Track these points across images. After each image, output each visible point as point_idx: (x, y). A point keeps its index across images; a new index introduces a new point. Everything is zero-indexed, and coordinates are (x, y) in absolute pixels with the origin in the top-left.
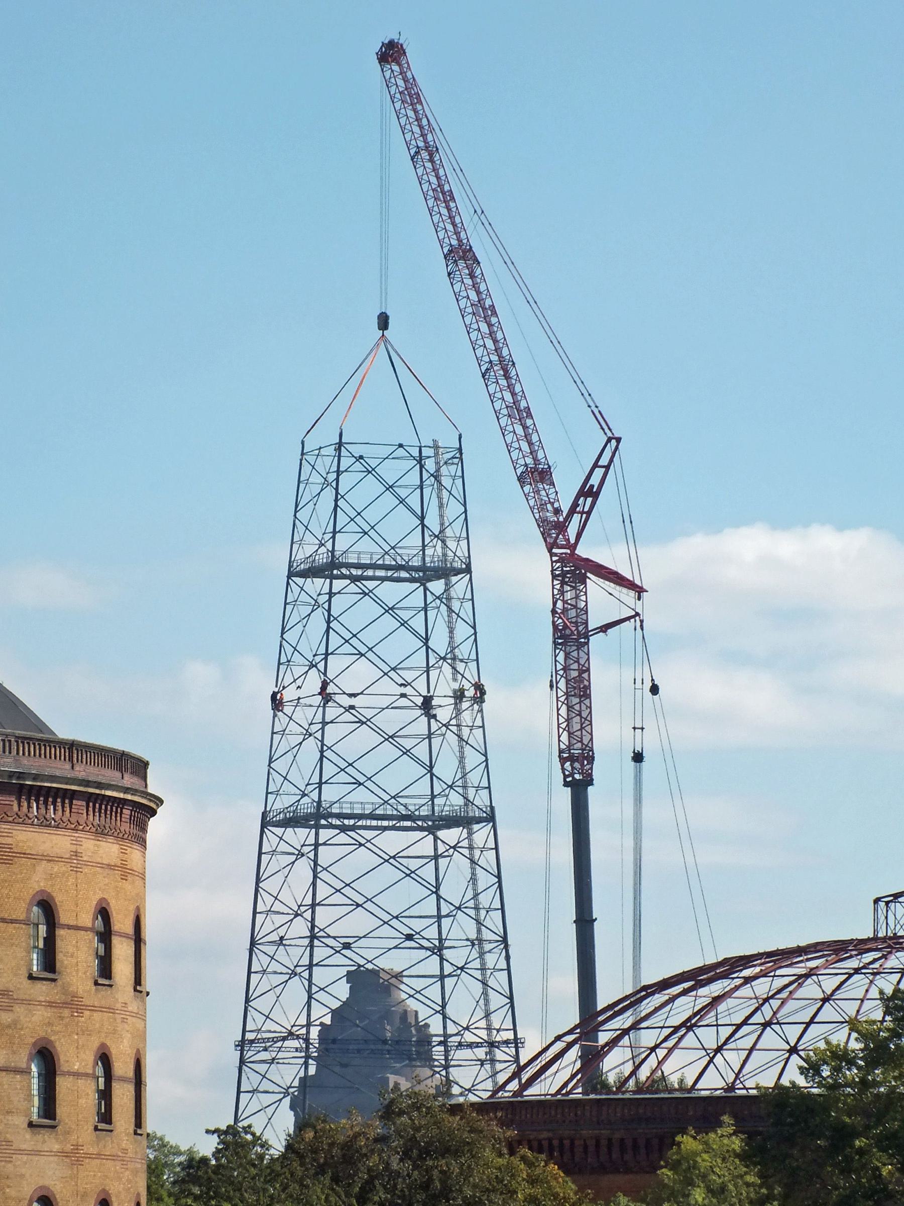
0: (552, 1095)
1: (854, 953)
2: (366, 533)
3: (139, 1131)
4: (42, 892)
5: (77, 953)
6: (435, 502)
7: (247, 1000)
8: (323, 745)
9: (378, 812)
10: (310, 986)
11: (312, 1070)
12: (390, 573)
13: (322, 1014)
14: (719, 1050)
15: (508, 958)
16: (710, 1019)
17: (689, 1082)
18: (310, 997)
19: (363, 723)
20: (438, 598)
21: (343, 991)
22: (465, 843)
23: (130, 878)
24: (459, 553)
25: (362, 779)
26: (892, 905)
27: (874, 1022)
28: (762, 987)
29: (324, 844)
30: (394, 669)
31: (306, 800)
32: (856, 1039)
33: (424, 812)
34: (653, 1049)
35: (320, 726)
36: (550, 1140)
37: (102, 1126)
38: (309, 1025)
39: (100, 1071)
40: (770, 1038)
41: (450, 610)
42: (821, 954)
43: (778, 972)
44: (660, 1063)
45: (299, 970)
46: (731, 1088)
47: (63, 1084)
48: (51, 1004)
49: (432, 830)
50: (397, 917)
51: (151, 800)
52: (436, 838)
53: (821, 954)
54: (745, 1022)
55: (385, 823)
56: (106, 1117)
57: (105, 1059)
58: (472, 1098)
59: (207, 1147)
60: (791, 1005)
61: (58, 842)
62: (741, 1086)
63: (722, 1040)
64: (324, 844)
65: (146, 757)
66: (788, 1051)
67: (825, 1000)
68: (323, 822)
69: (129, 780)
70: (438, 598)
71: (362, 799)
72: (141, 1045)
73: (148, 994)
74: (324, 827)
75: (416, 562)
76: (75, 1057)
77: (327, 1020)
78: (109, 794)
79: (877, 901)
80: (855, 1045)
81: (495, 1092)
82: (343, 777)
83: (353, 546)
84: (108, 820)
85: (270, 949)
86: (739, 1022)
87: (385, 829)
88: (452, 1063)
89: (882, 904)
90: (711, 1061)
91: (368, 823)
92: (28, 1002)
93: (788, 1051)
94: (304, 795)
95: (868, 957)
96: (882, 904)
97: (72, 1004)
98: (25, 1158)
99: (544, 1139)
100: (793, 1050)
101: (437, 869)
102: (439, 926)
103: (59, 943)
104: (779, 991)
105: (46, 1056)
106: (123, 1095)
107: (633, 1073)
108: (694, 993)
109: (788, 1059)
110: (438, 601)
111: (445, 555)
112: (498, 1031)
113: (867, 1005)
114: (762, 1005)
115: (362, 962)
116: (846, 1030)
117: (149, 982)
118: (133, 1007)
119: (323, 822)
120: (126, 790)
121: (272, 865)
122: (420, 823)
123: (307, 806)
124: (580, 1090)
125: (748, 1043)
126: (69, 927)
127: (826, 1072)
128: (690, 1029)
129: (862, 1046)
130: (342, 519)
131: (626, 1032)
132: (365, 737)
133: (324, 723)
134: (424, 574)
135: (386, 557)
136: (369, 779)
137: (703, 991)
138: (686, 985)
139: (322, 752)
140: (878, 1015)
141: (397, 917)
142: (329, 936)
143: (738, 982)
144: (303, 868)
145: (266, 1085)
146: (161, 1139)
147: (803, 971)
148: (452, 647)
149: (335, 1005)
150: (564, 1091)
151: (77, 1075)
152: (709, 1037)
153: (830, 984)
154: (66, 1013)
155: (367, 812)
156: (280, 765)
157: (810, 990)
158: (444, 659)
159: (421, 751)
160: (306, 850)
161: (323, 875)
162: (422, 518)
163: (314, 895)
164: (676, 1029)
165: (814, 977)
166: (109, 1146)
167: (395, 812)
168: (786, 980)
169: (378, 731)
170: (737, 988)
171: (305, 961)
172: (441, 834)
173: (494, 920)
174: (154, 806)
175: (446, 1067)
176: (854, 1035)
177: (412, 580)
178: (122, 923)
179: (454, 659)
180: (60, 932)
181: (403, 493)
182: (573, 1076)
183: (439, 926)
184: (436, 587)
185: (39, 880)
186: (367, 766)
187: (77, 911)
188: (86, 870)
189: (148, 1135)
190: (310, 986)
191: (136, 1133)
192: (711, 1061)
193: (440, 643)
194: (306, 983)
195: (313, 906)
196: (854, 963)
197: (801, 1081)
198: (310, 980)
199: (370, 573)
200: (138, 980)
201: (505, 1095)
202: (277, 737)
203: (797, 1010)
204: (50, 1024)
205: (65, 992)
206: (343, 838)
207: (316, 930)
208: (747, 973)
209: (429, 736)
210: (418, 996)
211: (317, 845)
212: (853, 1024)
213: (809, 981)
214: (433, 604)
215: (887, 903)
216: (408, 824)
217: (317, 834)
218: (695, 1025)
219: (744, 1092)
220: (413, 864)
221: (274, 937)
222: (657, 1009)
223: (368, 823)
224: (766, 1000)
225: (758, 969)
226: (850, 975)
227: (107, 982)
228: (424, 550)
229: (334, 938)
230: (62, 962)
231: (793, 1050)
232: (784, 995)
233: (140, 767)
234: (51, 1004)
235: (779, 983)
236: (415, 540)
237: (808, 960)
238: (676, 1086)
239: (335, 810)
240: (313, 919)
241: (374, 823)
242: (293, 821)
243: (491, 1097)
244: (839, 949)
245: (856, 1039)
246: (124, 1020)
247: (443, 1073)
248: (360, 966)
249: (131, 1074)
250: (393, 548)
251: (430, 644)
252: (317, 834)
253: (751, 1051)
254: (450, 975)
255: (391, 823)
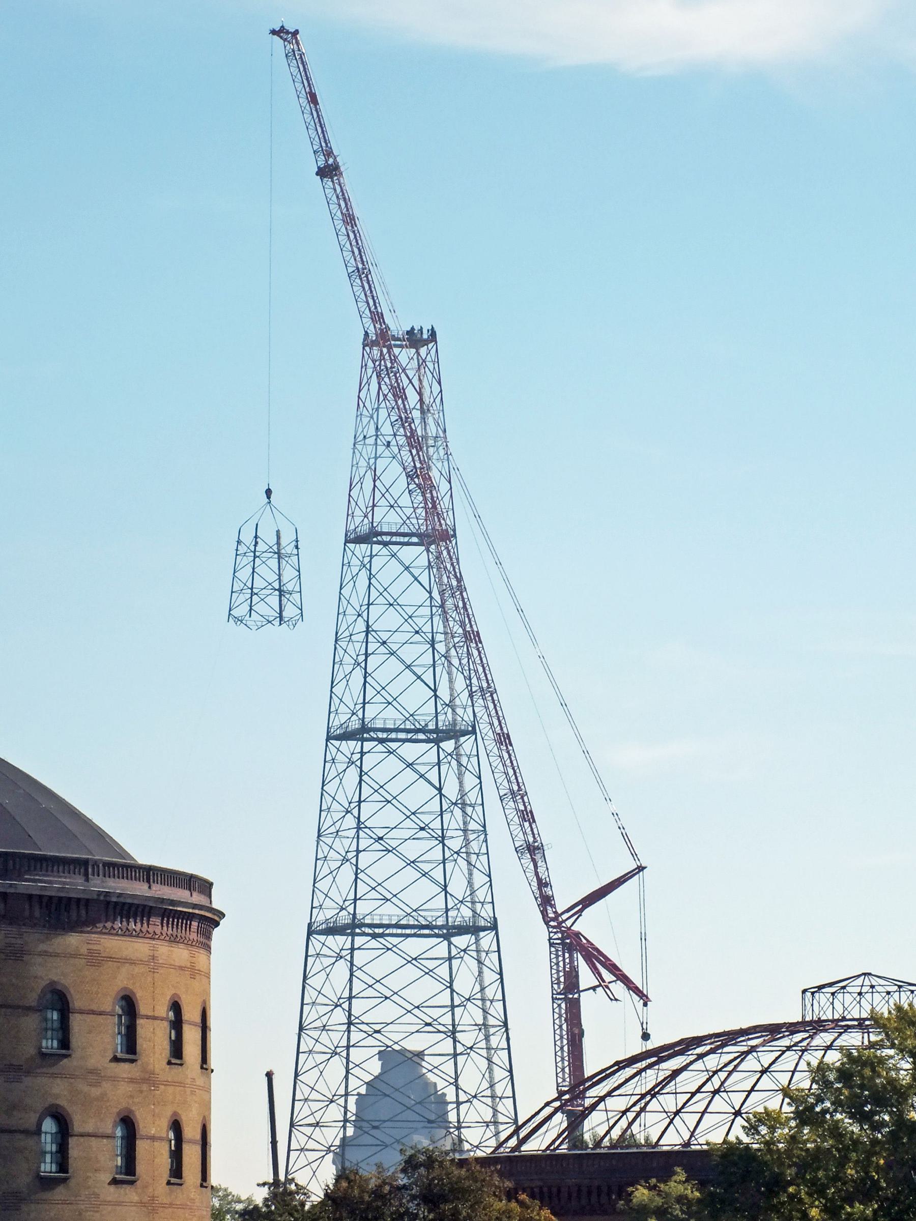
0: (543, 1151)
1: (787, 1033)
2: (390, 703)
3: (204, 1184)
4: (125, 989)
5: (154, 1037)
6: (445, 676)
7: (296, 1075)
8: (357, 868)
9: (402, 922)
10: (348, 1063)
11: (350, 1131)
12: (410, 736)
13: (357, 1085)
14: (677, 1113)
15: (508, 1039)
16: (670, 1088)
17: (655, 1140)
18: (348, 1072)
19: (389, 851)
20: (449, 754)
21: (375, 1067)
22: (473, 947)
23: (198, 977)
24: (466, 718)
25: (389, 896)
26: (817, 995)
27: (803, 1090)
28: (712, 1062)
29: (359, 948)
30: (413, 814)
31: (344, 913)
32: (789, 1104)
33: (440, 922)
34: (624, 1113)
35: (355, 853)
36: (541, 1188)
37: (173, 1180)
38: (347, 1094)
39: (171, 1135)
40: (719, 1103)
41: (460, 764)
42: (759, 1034)
43: (726, 1049)
44: (630, 1124)
45: (338, 1050)
46: (687, 1144)
47: (141, 1146)
48: (132, 1081)
49: (447, 937)
50: (418, 1007)
51: (214, 914)
52: (450, 943)
53: (759, 1034)
54: (698, 1091)
55: (408, 931)
56: (177, 1171)
57: (176, 1126)
58: (479, 1154)
59: (260, 1196)
60: (735, 1076)
61: (138, 948)
62: (695, 1142)
63: (680, 1106)
64: (359, 948)
65: (211, 880)
66: (733, 1114)
67: (764, 1072)
68: (358, 931)
69: (197, 898)
70: (449, 754)
71: (389, 913)
72: (206, 1114)
73: (212, 1071)
74: (359, 935)
75: (431, 726)
76: (153, 1124)
77: (363, 1090)
78: (182, 909)
79: (804, 991)
80: (788, 1109)
81: (497, 1148)
82: (373, 894)
83: (381, 715)
84: (179, 930)
85: (315, 1034)
86: (693, 1090)
87: (408, 936)
88: (463, 1125)
89: (808, 994)
90: (671, 1122)
91: (395, 931)
92: (114, 1079)
93: (733, 1114)
94: (342, 909)
95: (798, 1037)
96: (808, 994)
97: (149, 1079)
98: (110, 1208)
99: (536, 1187)
100: (738, 1113)
101: (451, 968)
102: (453, 1014)
103: (139, 1029)
104: (726, 1065)
105: (128, 1123)
106: (191, 1155)
107: (608, 1132)
108: (657, 1067)
109: (733, 1120)
110: (449, 757)
111: (454, 720)
112: (500, 1098)
113: (797, 1076)
114: (713, 1076)
115: (390, 1043)
116: (781, 1097)
117: (214, 1061)
118: (200, 1082)
119: (358, 931)
120: (195, 906)
121: (315, 966)
122: (436, 931)
123: (344, 918)
124: (564, 1146)
125: (701, 1107)
126: (148, 1017)
127: (764, 1130)
128: (653, 1096)
129: (793, 1109)
130: (370, 693)
131: (602, 1099)
132: (392, 862)
133: (358, 851)
134: (438, 736)
135: (407, 722)
136: (395, 896)
137: (663, 1065)
138: (650, 1061)
139: (356, 874)
140: (806, 1084)
141: (418, 1007)
142: (363, 1023)
143: (692, 1058)
144: (342, 968)
145: (311, 1145)
146: (226, 1190)
147: (745, 1049)
148: (463, 794)
149: (368, 1078)
150: (552, 1148)
151: (153, 1138)
152: (669, 1102)
153: (767, 1059)
154: (145, 1087)
155: (394, 922)
156: (323, 885)
157: (751, 1063)
158: (455, 804)
159: (438, 874)
160: (344, 953)
161: (358, 973)
162: (435, 691)
163: (351, 989)
164: (643, 1096)
165: (754, 1054)
166: (180, 1196)
167: (416, 923)
168: (732, 1056)
169: (401, 856)
170: (691, 1063)
171: (344, 1043)
172: (453, 940)
173: (496, 1009)
174: (216, 918)
175: (459, 1128)
176: (787, 1100)
177: (428, 741)
178: (191, 1014)
179: (464, 804)
180: (140, 1022)
181: (419, 671)
182: (559, 1136)
183: (453, 1014)
184: (448, 746)
185: (122, 980)
186: (394, 886)
187: (154, 1006)
188: (161, 971)
189: (212, 1187)
190: (348, 1063)
191: (202, 1186)
192: (671, 1122)
193: (451, 791)
194: (345, 1061)
195: (350, 998)
196: (786, 1042)
197: (746, 1140)
198: (347, 1058)
199: (393, 735)
200: (204, 1059)
201: (505, 1151)
202: (320, 863)
203: (740, 1081)
204: (132, 1097)
205: (144, 1070)
206: (374, 943)
207: (353, 1018)
208: (700, 1050)
209: (444, 861)
210: (435, 1071)
211: (352, 949)
212: (786, 1092)
213: (750, 1057)
214: (445, 760)
215: (813, 993)
216: (426, 932)
217: (353, 941)
218: (658, 1093)
219: (698, 1147)
220: (431, 964)
221: (318, 1024)
222: (627, 1081)
223: (395, 931)
224: (715, 1072)
225: (708, 1047)
226: (784, 1052)
227: (178, 1061)
228: (436, 717)
229: (367, 1024)
230: (142, 1046)
231: (738, 1113)
232: (730, 1068)
233: (206, 887)
234: (132, 1081)
235: (726, 1058)
236: (430, 708)
237: (749, 1039)
238: (643, 1142)
239: (368, 921)
240: (350, 1009)
241: (399, 931)
242: (332, 930)
243: (493, 1153)
244: (773, 1031)
245: (789, 1104)
246: (193, 1093)
247: (456, 1133)
248: (388, 1047)
249: (198, 1137)
250: (411, 715)
251: (443, 792)
252: (353, 941)
253: (703, 1113)
254: (461, 1054)
255: (413, 931)
